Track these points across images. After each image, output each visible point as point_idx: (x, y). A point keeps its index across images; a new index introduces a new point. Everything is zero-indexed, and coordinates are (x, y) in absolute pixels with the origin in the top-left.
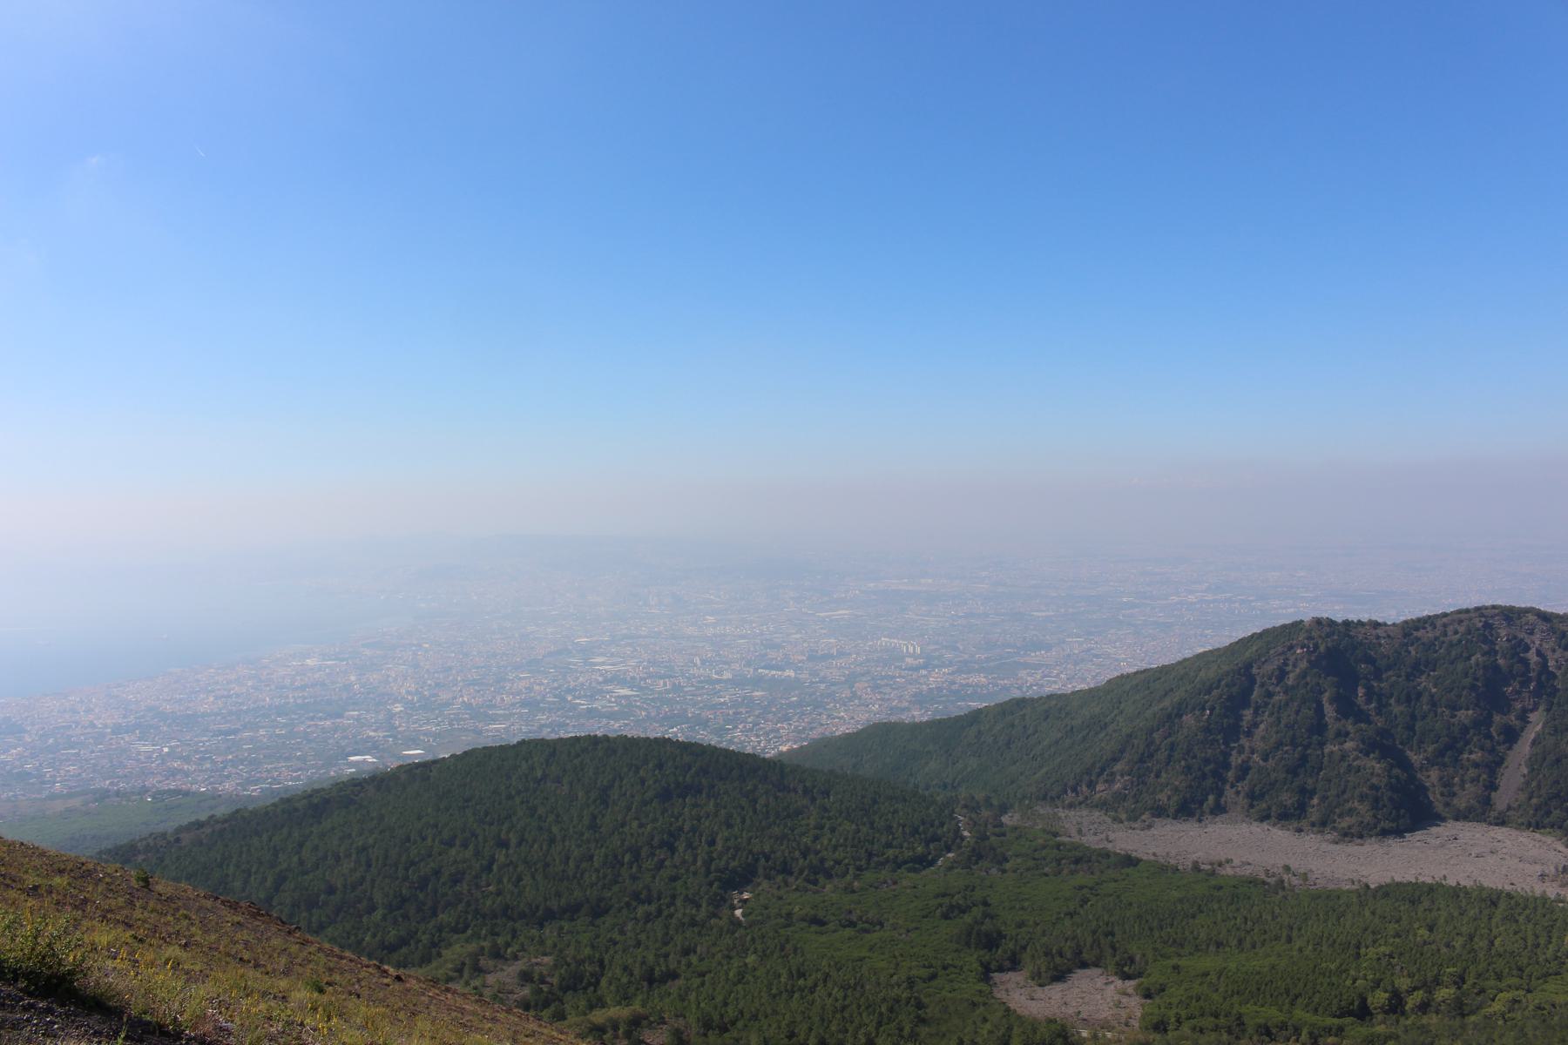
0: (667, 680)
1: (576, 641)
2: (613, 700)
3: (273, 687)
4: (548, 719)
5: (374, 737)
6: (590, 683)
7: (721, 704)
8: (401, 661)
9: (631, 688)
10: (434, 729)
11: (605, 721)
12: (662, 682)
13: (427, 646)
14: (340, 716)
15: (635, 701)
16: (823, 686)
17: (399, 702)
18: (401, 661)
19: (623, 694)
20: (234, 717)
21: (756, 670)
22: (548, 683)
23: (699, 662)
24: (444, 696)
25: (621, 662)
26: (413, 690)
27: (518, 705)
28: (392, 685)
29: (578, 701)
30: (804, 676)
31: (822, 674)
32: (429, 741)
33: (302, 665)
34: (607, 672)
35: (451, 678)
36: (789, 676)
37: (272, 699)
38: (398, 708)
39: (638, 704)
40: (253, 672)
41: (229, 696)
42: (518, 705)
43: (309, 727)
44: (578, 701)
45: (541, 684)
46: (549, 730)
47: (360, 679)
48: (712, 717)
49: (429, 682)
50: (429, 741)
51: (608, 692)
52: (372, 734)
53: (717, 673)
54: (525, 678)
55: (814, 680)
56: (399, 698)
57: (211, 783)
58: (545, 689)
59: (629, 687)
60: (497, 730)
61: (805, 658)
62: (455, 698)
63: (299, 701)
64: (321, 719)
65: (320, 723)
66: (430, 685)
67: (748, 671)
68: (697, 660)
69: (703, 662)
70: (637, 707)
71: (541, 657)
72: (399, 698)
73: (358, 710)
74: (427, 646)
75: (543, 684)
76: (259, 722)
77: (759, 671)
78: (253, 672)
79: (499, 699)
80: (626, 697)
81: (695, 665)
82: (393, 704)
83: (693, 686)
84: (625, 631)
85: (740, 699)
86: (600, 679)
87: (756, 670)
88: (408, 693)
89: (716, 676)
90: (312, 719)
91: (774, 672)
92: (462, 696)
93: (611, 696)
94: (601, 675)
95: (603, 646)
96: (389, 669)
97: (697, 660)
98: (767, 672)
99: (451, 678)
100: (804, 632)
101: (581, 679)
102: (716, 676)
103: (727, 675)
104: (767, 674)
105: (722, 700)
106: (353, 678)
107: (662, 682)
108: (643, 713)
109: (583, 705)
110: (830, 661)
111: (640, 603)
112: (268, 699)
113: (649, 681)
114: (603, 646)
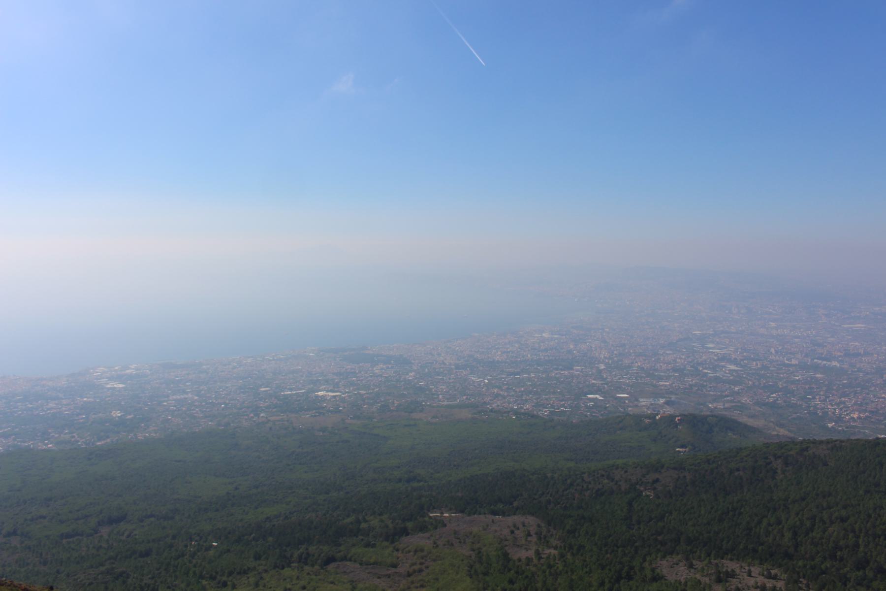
0: (758, 362)
1: (694, 333)
2: (727, 372)
3: (530, 349)
4: (692, 381)
5: (596, 384)
6: (710, 360)
7: (797, 380)
8: (595, 338)
9: (736, 364)
10: (627, 381)
11: (727, 386)
12: (754, 363)
13: (607, 330)
14: (572, 369)
15: (742, 374)
16: (861, 375)
17: (602, 363)
18: (595, 338)
19: (732, 369)
20: (514, 365)
21: (812, 360)
22: (685, 358)
23: (774, 352)
24: (627, 362)
25: (725, 348)
26: (608, 356)
27: (671, 371)
28: (595, 352)
29: (706, 371)
30: (846, 366)
31: (858, 366)
32: (628, 389)
33: (541, 336)
34: (718, 354)
35: (626, 351)
36: (836, 366)
37: (531, 356)
38: (602, 367)
39: (744, 376)
40: (516, 339)
41: (508, 352)
42: (671, 371)
43: (557, 374)
44: (706, 371)
45: (681, 358)
46: (697, 388)
47: (576, 348)
48: (795, 388)
49: (615, 352)
50: (628, 389)
51: (723, 367)
52: (593, 381)
53: (787, 360)
54: (670, 354)
55: (854, 370)
56: (601, 360)
57: (518, 404)
58: (684, 362)
59: (734, 365)
60: (665, 386)
61: (842, 354)
62: (632, 363)
63: (547, 358)
64: (562, 370)
65: (562, 372)
66: (616, 354)
67: (808, 360)
68: (772, 350)
69: (776, 352)
70: (744, 378)
71: (675, 342)
72: (601, 360)
73: (580, 366)
74: (607, 330)
75: (682, 358)
76: (529, 368)
77: (815, 361)
78: (516, 339)
79: (659, 366)
80: (736, 371)
81: (772, 353)
82: (598, 364)
83: (774, 367)
84: (721, 329)
85: (809, 379)
86: (716, 358)
87: (812, 360)
88: (605, 358)
89: (787, 362)
90: (557, 369)
91: (825, 362)
92: (636, 362)
93: (725, 369)
94: (715, 355)
95: (711, 337)
96: (590, 342)
97: (772, 350)
98: (820, 361)
99: (626, 351)
100: (836, 337)
101: (704, 357)
102: (787, 362)
103: (794, 362)
104: (821, 363)
105: (797, 378)
106: (572, 347)
107: (754, 363)
108: (750, 383)
109: (709, 373)
110: (860, 358)
111: (727, 312)
112: (529, 356)
113: (745, 361)
114: (711, 337)
